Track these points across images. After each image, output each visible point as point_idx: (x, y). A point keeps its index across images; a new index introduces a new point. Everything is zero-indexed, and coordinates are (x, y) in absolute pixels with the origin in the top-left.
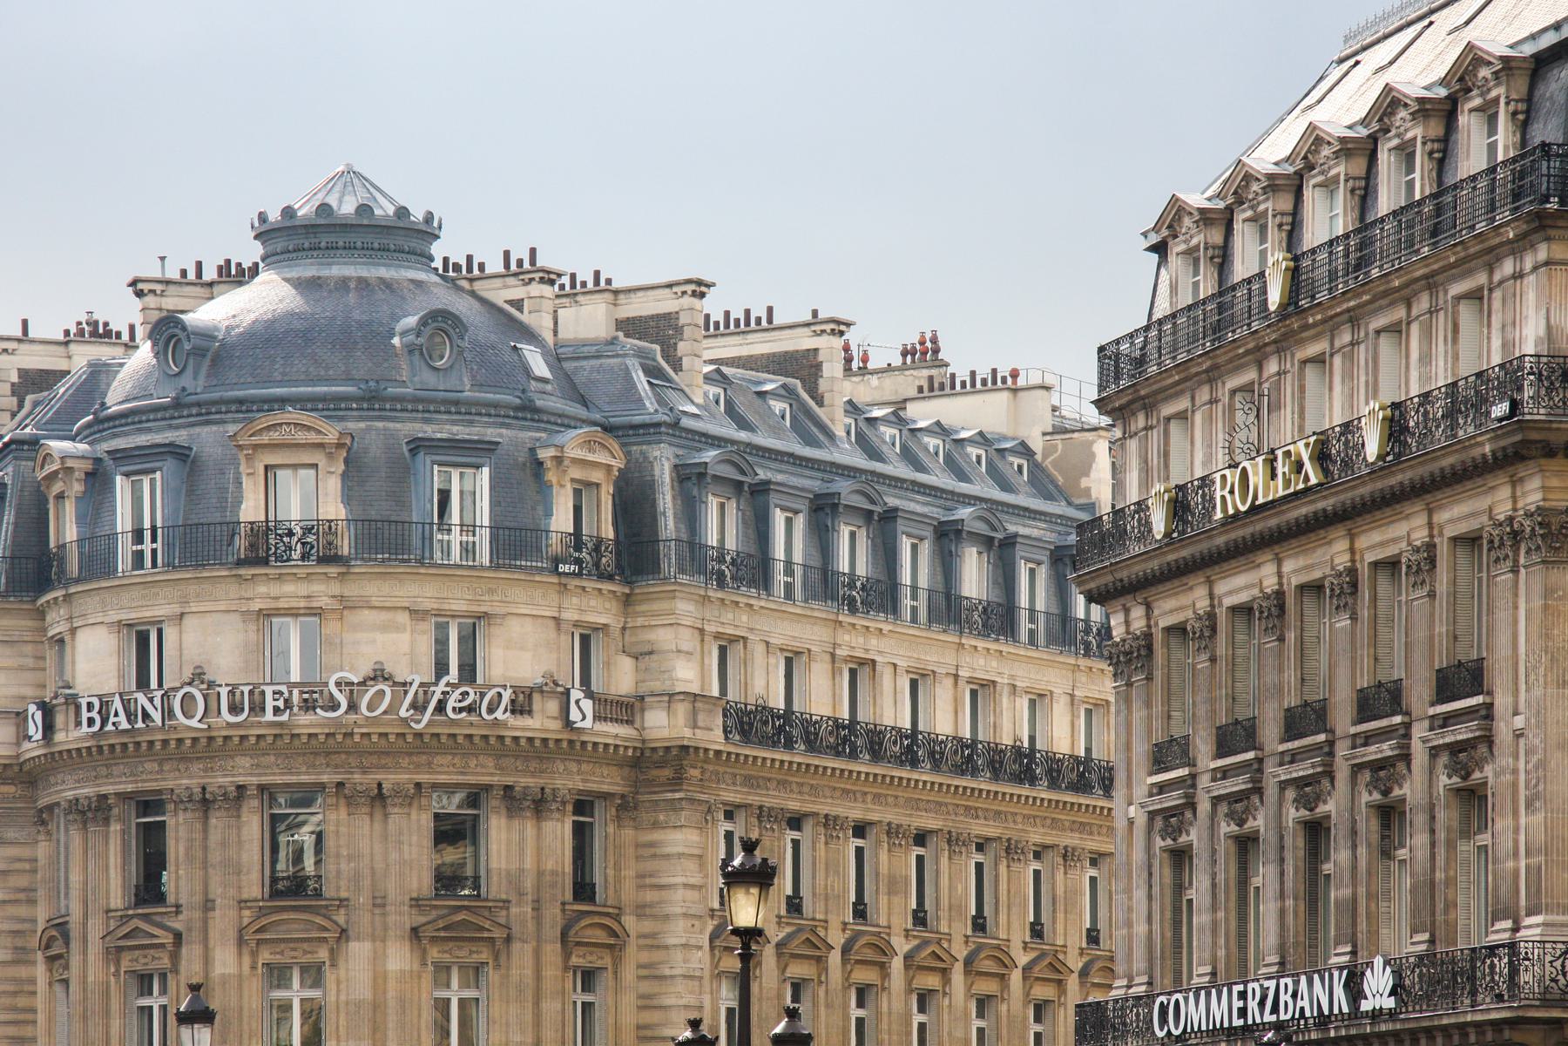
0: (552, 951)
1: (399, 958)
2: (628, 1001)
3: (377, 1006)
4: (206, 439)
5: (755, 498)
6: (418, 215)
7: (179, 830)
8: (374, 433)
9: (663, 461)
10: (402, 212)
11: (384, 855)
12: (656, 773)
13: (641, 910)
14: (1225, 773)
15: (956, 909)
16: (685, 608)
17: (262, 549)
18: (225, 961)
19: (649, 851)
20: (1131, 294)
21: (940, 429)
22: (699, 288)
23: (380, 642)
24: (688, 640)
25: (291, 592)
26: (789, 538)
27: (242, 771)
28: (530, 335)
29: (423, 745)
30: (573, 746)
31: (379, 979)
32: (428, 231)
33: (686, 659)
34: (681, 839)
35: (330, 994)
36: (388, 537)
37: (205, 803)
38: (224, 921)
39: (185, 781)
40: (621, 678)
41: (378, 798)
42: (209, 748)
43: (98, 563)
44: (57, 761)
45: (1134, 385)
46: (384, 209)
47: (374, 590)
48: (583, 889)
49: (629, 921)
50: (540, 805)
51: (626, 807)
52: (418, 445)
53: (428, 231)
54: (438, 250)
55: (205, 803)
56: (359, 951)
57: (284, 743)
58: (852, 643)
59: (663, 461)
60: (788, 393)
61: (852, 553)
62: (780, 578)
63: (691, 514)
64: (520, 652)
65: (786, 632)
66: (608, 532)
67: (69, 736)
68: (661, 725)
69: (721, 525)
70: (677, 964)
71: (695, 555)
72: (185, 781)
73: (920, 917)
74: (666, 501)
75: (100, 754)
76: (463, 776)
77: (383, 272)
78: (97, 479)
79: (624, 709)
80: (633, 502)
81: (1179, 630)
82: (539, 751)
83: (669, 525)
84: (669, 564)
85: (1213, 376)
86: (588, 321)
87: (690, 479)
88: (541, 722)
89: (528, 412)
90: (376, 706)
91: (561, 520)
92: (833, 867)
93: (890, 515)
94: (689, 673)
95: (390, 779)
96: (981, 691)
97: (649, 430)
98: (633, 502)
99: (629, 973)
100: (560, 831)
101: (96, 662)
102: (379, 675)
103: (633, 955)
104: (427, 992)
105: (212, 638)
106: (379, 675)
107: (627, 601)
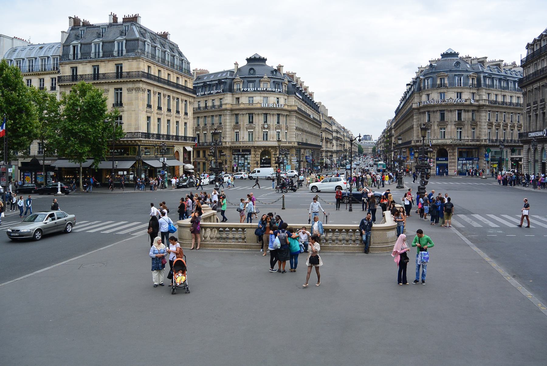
0: (469, 126)
1: (453, 127)
2: (478, 131)
3: (451, 132)
9: (482, 76)
11: (452, 117)
12: (480, 107)
13: (479, 122)
14: (541, 105)
15: (516, 120)
16: (484, 90)
18: (436, 127)
19: (480, 116)
20: (524, 53)
21: (514, 71)
22: (486, 58)
24: (484, 94)
26: (496, 83)
27: (437, 108)
28: (468, 63)
29: (455, 105)
30: (471, 105)
31: (451, 129)
32: (458, 54)
34: (483, 114)
36: (452, 85)
37: (434, 112)
38: (436, 123)
39: (432, 110)
40: (477, 98)
41: (451, 111)
42: (434, 106)
45: (525, 64)
46: (453, 52)
47: (450, 90)
48: (473, 119)
49: (478, 123)
50: (468, 111)
51: (478, 111)
52: (455, 75)
53: (458, 54)
54: (459, 56)
55: (434, 112)
56: (449, 126)
58: (503, 93)
59: (482, 76)
60: (497, 68)
61: (503, 84)
62: (495, 87)
63: (485, 81)
65: (496, 93)
66: (476, 83)
68: (481, 103)
70: (483, 127)
71: (485, 85)
72: (432, 110)
73: (512, 121)
74: (482, 79)
75: (425, 107)
76: (461, 108)
79: (478, 101)
81: (529, 91)
84: (482, 86)
85: (532, 62)
87: (485, 77)
88: (468, 103)
92: (501, 117)
93: (508, 80)
94: (485, 97)
95: (452, 109)
97: (480, 72)
99: (478, 128)
100: (470, 114)
102: (451, 98)
103: (478, 126)
104: (456, 130)
106: (451, 98)
107: (478, 90)
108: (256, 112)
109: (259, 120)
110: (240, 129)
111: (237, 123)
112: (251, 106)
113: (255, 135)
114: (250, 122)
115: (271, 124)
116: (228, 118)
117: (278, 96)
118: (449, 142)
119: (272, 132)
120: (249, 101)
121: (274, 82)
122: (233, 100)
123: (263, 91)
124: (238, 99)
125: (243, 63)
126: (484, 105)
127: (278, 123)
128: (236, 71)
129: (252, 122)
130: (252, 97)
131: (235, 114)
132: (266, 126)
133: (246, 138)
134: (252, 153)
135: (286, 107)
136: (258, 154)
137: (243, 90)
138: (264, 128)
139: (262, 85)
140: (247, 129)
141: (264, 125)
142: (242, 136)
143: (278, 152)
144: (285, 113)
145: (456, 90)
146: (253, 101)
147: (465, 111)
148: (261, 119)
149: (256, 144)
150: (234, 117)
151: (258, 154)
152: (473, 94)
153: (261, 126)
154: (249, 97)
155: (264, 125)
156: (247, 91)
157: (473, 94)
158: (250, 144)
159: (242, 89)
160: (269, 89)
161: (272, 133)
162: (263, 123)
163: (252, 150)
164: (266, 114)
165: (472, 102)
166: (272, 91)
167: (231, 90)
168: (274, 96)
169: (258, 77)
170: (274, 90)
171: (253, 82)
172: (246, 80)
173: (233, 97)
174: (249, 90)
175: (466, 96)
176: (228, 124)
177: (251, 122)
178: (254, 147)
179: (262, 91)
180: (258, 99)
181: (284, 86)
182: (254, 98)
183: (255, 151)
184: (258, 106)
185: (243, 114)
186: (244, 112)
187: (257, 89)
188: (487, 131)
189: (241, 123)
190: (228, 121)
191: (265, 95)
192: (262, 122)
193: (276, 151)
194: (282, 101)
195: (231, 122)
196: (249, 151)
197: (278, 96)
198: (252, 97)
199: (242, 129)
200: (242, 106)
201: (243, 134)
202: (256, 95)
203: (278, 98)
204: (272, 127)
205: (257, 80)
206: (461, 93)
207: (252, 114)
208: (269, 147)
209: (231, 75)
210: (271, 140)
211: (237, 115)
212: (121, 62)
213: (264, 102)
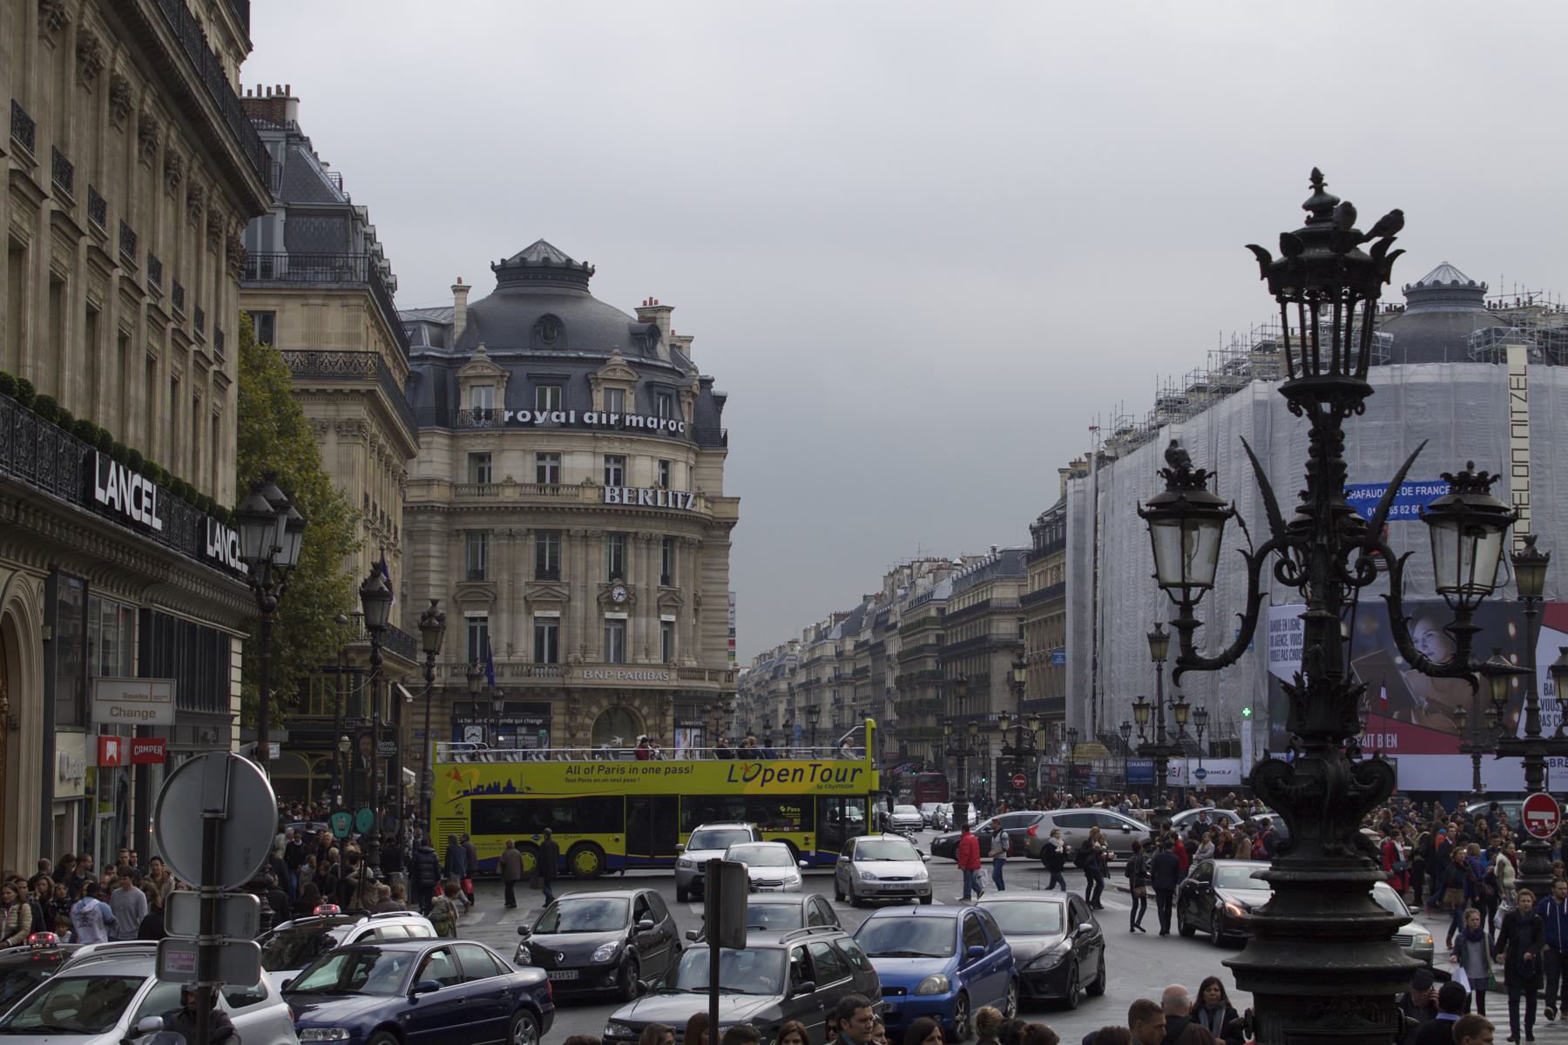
6: (1478, 283)
10: (1472, 283)
32: (1482, 290)
53: (1482, 290)
54: (1486, 298)
77: (1462, 309)
108: (577, 525)
109: (586, 566)
110: (493, 603)
111: (477, 574)
112: (548, 499)
113: (570, 636)
114: (541, 573)
115: (642, 585)
116: (434, 549)
117: (666, 454)
119: (643, 621)
120: (541, 471)
121: (650, 386)
122: (454, 465)
123: (609, 426)
124: (481, 459)
125: (484, 286)
127: (666, 579)
128: (460, 326)
129: (554, 573)
130: (556, 456)
131: (470, 533)
132: (618, 594)
133: (526, 648)
134: (558, 719)
135: (701, 507)
136: (583, 727)
137: (513, 420)
138: (612, 604)
139: (599, 398)
140: (529, 606)
141: (609, 589)
142: (505, 639)
143: (670, 720)
144: (693, 535)
146: (555, 470)
148: (599, 559)
149: (581, 678)
150: (460, 546)
151: (583, 727)
153: (595, 593)
154: (541, 456)
155: (609, 589)
156: (531, 423)
158: (546, 678)
159: (507, 415)
160: (633, 420)
161: (645, 627)
162: (604, 579)
163: (558, 706)
164: (621, 537)
166: (646, 429)
167: (446, 416)
168: (652, 450)
169: (580, 359)
170: (652, 423)
171: (558, 381)
172: (520, 371)
173: (453, 450)
174: (540, 419)
176: (434, 578)
177: (547, 571)
178: (567, 691)
179: (600, 426)
180: (581, 464)
181: (685, 407)
182: (567, 462)
183: (572, 713)
184: (590, 496)
185: (511, 535)
186: (518, 524)
187: (579, 418)
189: (498, 576)
190: (434, 563)
191: (616, 449)
192: (600, 575)
193: (664, 715)
194: (680, 480)
195: (445, 570)
196: (544, 710)
197: (666, 454)
198: (556, 456)
199: (504, 603)
200: (510, 495)
201: (513, 630)
202: (577, 445)
203: (665, 464)
204: (643, 599)
205: (578, 372)
207: (555, 534)
208: (635, 693)
209: (438, 342)
210: (642, 659)
211: (478, 537)
212: (269, 304)
213: (607, 482)
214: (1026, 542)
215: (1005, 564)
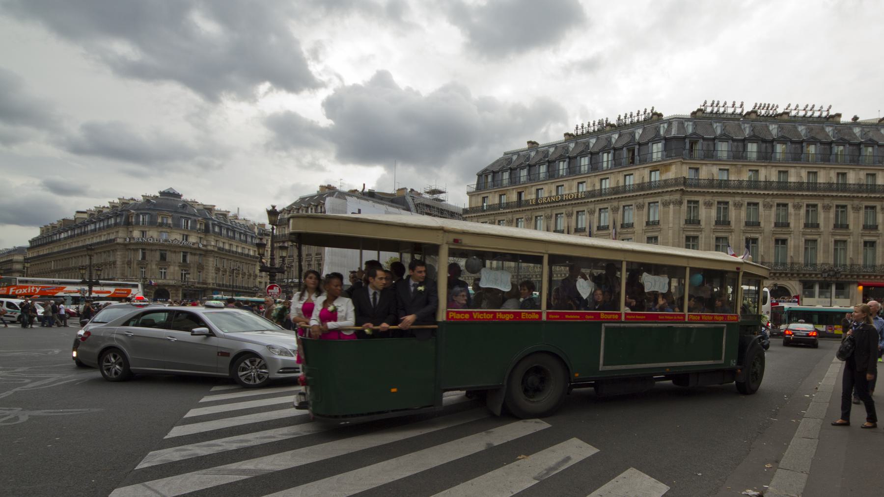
1: (177, 268)
4: (153, 213)
5: (220, 227)
7: (148, 253)
8: (176, 215)
9: (210, 222)
17: (161, 225)
23: (176, 237)
25: (164, 230)
30: (199, 249)
33: (212, 243)
35: (168, 271)
36: (177, 226)
40: (205, 243)
42: (152, 244)
43: (137, 223)
44: (130, 244)
57: (162, 245)
63: (213, 228)
64: (193, 239)
67: (132, 241)
68: (210, 248)
69: (217, 229)
76: (186, 250)
78: (138, 216)
79: (204, 245)
80: (207, 226)
82: (195, 249)
83: (211, 228)
86: (201, 207)
87: (214, 225)
88: (196, 246)
89: (195, 215)
90: (175, 243)
91: (198, 226)
96: (243, 248)
98: (207, 226)
101: (136, 234)
105: (153, 234)
118: (172, 282)
126: (213, 251)
145: (182, 232)
147: (191, 254)
152: (201, 238)
157: (201, 238)
165: (201, 246)
175: (193, 239)
188: (214, 275)
206: (187, 236)
214: (28, 244)
215: (19, 250)
